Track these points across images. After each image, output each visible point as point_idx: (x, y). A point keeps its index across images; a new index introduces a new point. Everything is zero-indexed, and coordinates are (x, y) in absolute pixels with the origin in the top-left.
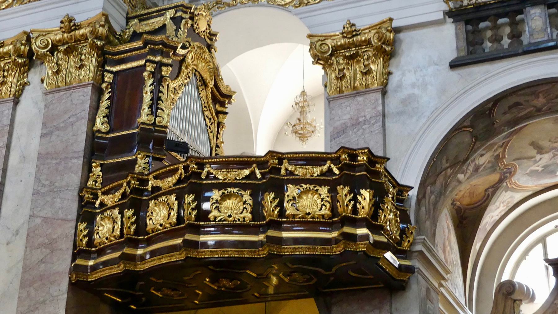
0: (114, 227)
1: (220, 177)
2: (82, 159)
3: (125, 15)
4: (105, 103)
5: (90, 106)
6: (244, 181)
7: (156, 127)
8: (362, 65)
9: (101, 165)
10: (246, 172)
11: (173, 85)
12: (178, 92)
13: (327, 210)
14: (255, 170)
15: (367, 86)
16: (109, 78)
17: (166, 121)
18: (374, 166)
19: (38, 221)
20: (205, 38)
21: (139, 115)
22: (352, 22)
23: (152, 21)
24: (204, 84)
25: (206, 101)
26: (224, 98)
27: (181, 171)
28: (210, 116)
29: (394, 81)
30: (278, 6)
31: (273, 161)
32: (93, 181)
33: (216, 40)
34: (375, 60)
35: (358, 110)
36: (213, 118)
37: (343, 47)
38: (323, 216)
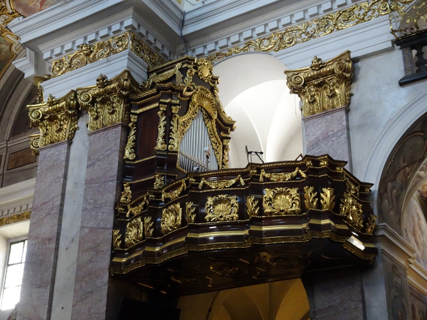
0: (138, 232)
1: (213, 187)
2: (116, 181)
3: (146, 71)
4: (132, 138)
5: (120, 141)
8: (329, 91)
9: (130, 185)
10: (233, 182)
11: (182, 120)
13: (297, 206)
14: (239, 179)
15: (333, 107)
16: (134, 119)
17: (176, 147)
18: (335, 169)
19: (86, 230)
20: (208, 82)
21: (156, 144)
22: (318, 57)
23: (166, 73)
24: (210, 117)
25: (212, 130)
26: (227, 126)
27: (184, 184)
28: (216, 141)
29: (354, 99)
30: (263, 52)
31: (253, 171)
32: (125, 198)
33: (218, 83)
34: (338, 85)
35: (327, 126)
36: (219, 143)
37: (313, 78)
38: (294, 212)
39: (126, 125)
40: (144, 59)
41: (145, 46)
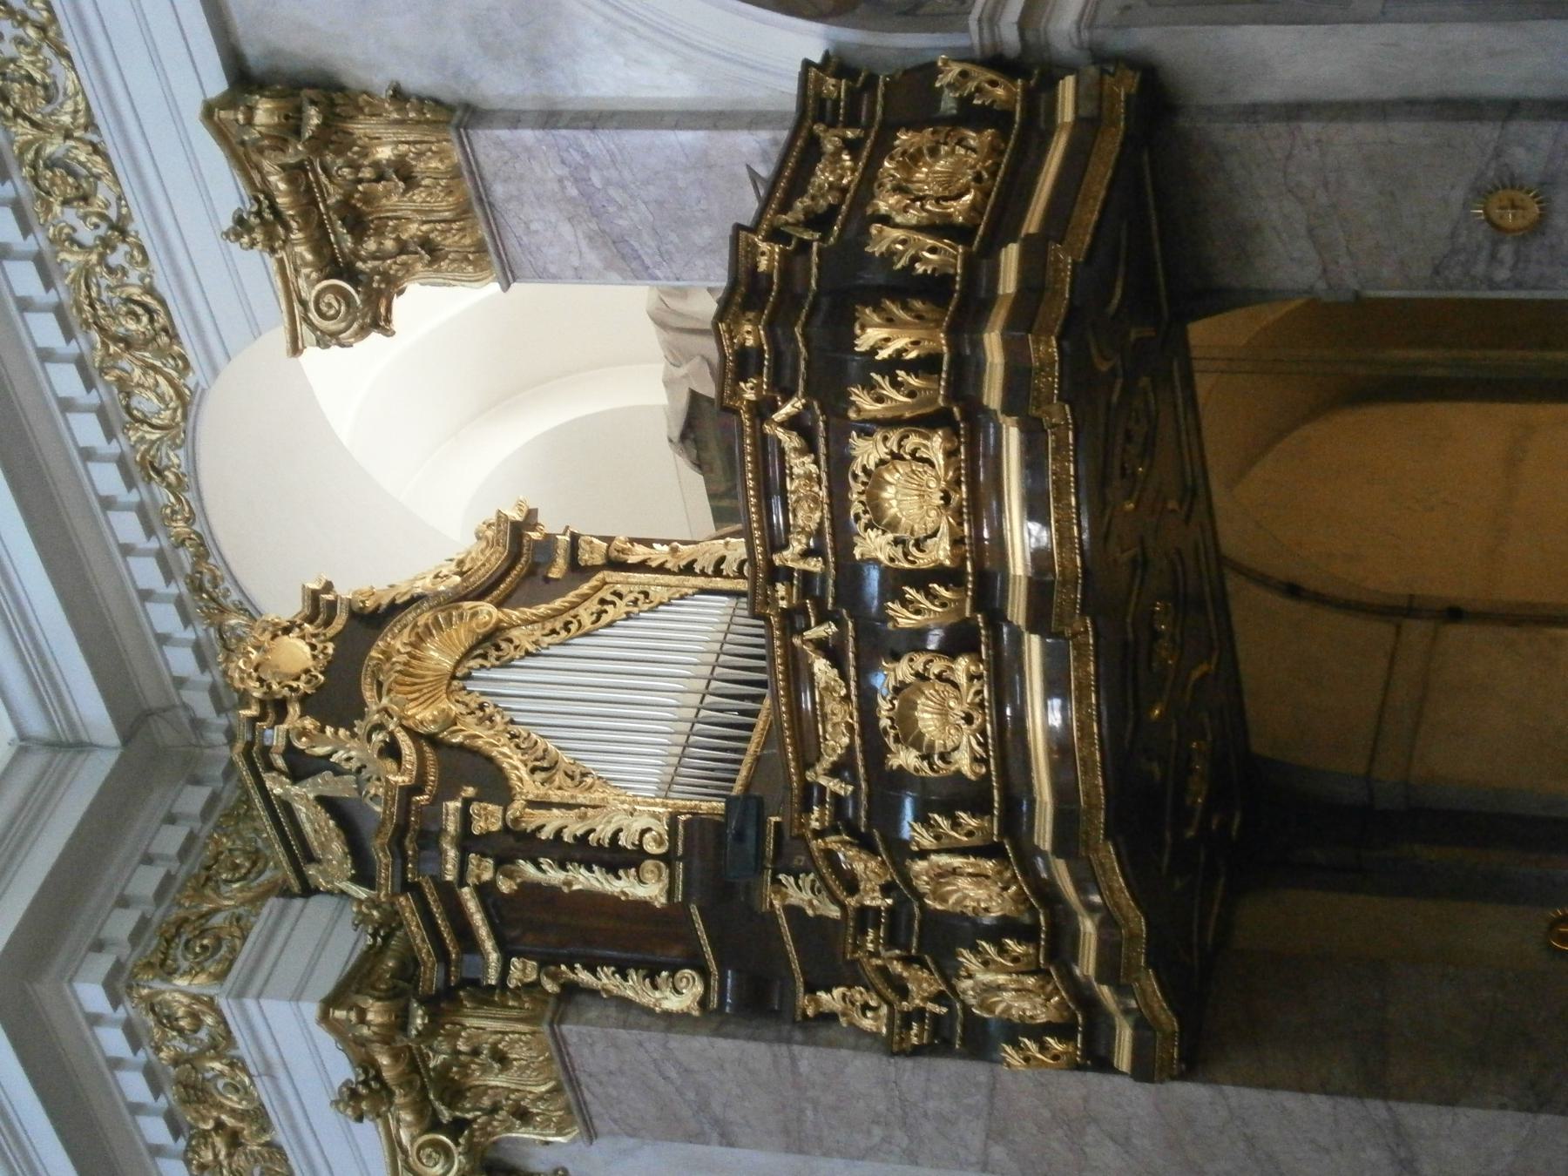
1: (846, 740)
2: (796, 1048)
3: (298, 903)
4: (607, 979)
5: (624, 1027)
6: (852, 671)
7: (676, 852)
8: (380, 187)
9: (811, 989)
10: (823, 668)
11: (527, 785)
12: (540, 753)
13: (929, 444)
14: (811, 640)
15: (455, 174)
16: (522, 970)
17: (652, 823)
18: (769, 276)
19: (998, 1152)
20: (331, 640)
21: (643, 905)
22: (227, 223)
23: (308, 828)
24: (490, 642)
25: (549, 626)
26: (520, 545)
27: (832, 842)
28: (593, 605)
29: (417, 79)
30: (191, 420)
31: (783, 598)
32: (864, 1015)
33: (328, 587)
34: (356, 149)
35: (538, 199)
36: (597, 589)
37: (320, 243)
38: (950, 454)
39: (552, 1000)
40: (241, 910)
41: (180, 905)
